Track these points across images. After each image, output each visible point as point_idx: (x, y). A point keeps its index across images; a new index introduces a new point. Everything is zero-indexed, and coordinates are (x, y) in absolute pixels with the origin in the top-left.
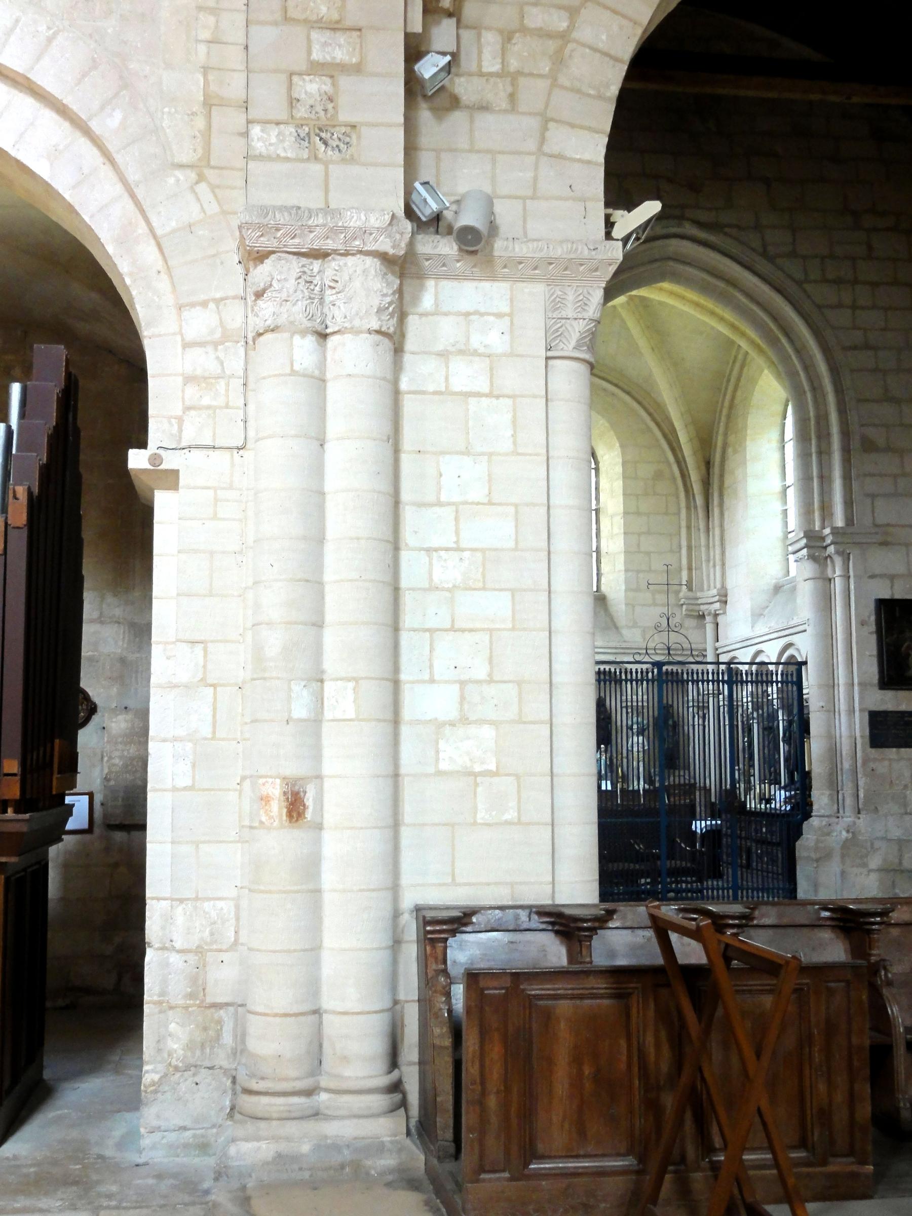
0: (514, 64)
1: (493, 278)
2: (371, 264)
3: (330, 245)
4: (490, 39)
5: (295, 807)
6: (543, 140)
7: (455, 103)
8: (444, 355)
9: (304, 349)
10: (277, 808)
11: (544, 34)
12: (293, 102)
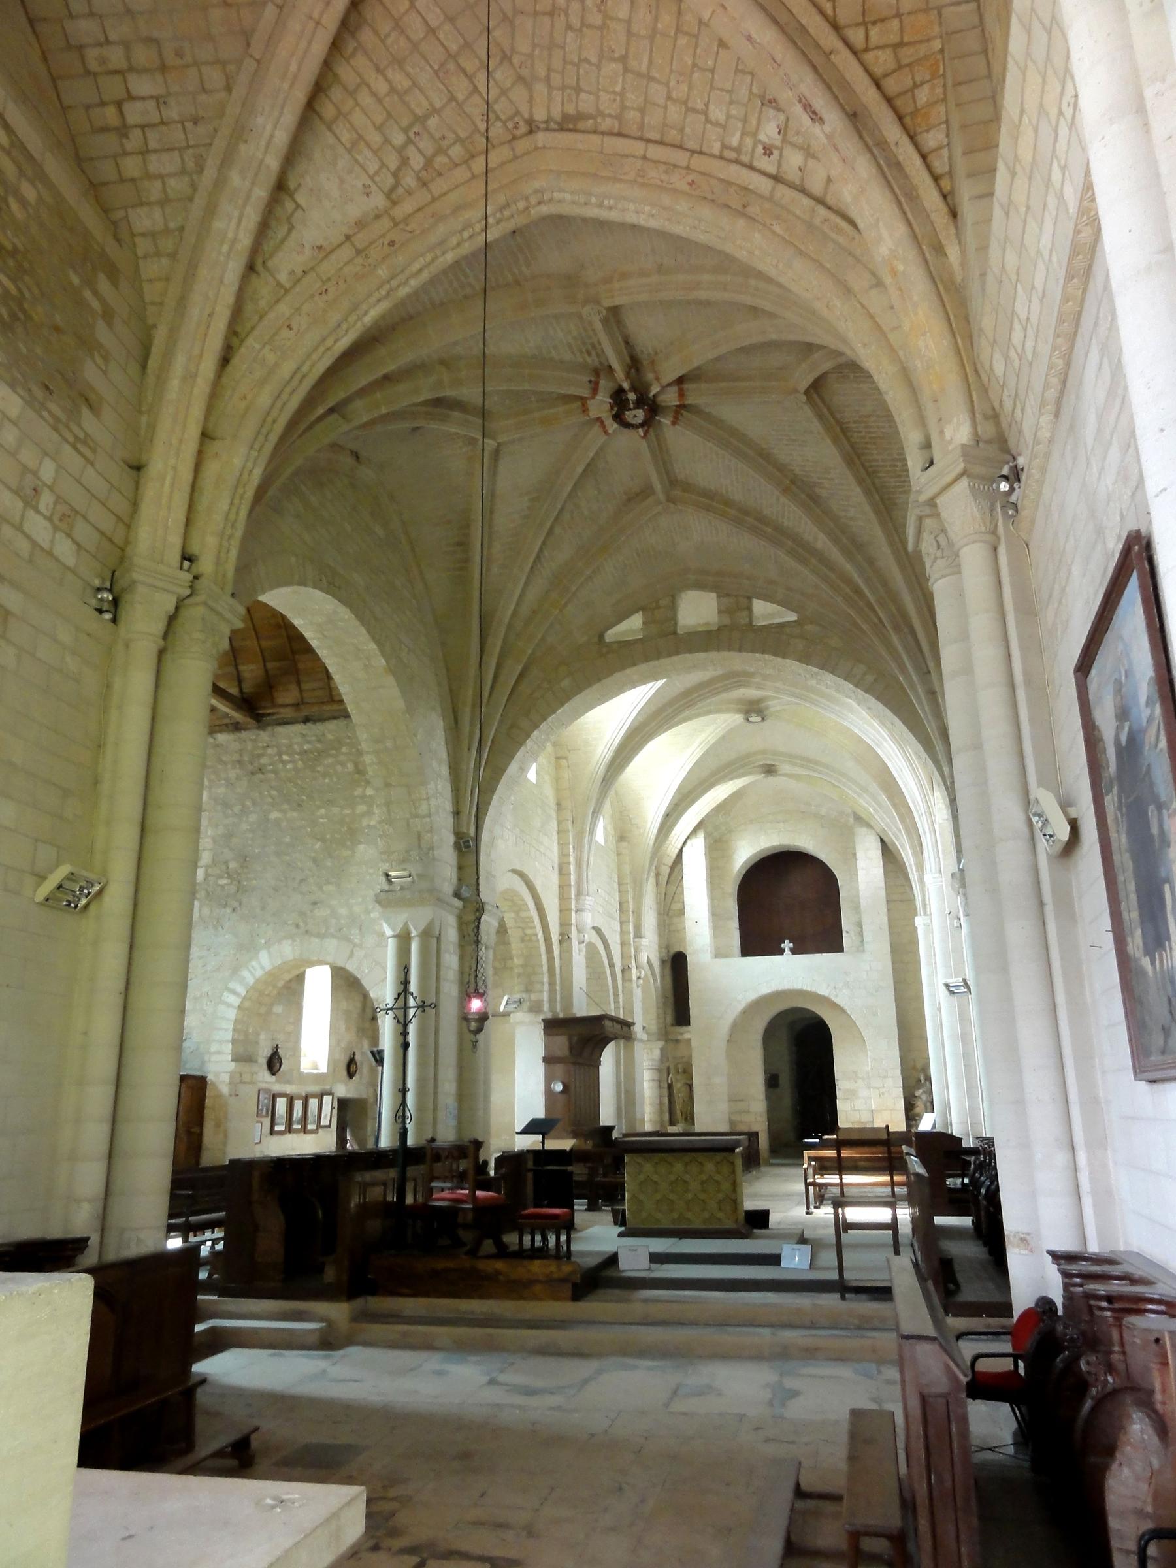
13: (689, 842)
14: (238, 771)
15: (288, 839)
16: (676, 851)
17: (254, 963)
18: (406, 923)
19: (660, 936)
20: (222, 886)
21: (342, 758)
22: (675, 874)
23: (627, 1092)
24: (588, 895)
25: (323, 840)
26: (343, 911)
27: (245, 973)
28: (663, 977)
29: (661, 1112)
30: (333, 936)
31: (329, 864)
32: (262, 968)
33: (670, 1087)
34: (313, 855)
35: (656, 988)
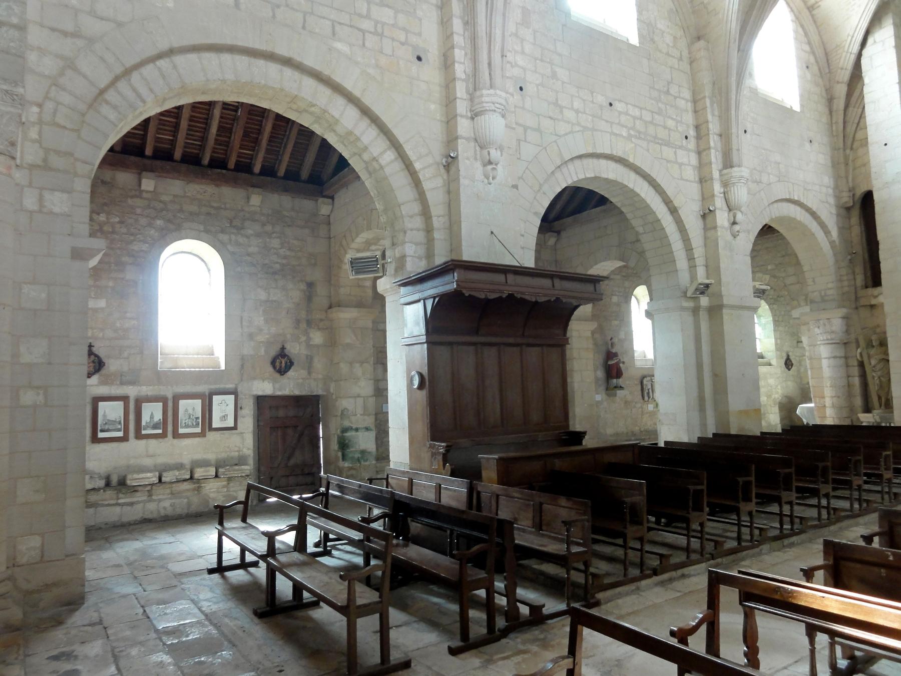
13: (870, 40)
16: (853, 58)
19: (837, 178)
22: (856, 94)
23: (715, 375)
24: (492, 86)
28: (843, 229)
29: (850, 395)
33: (861, 365)
35: (832, 243)
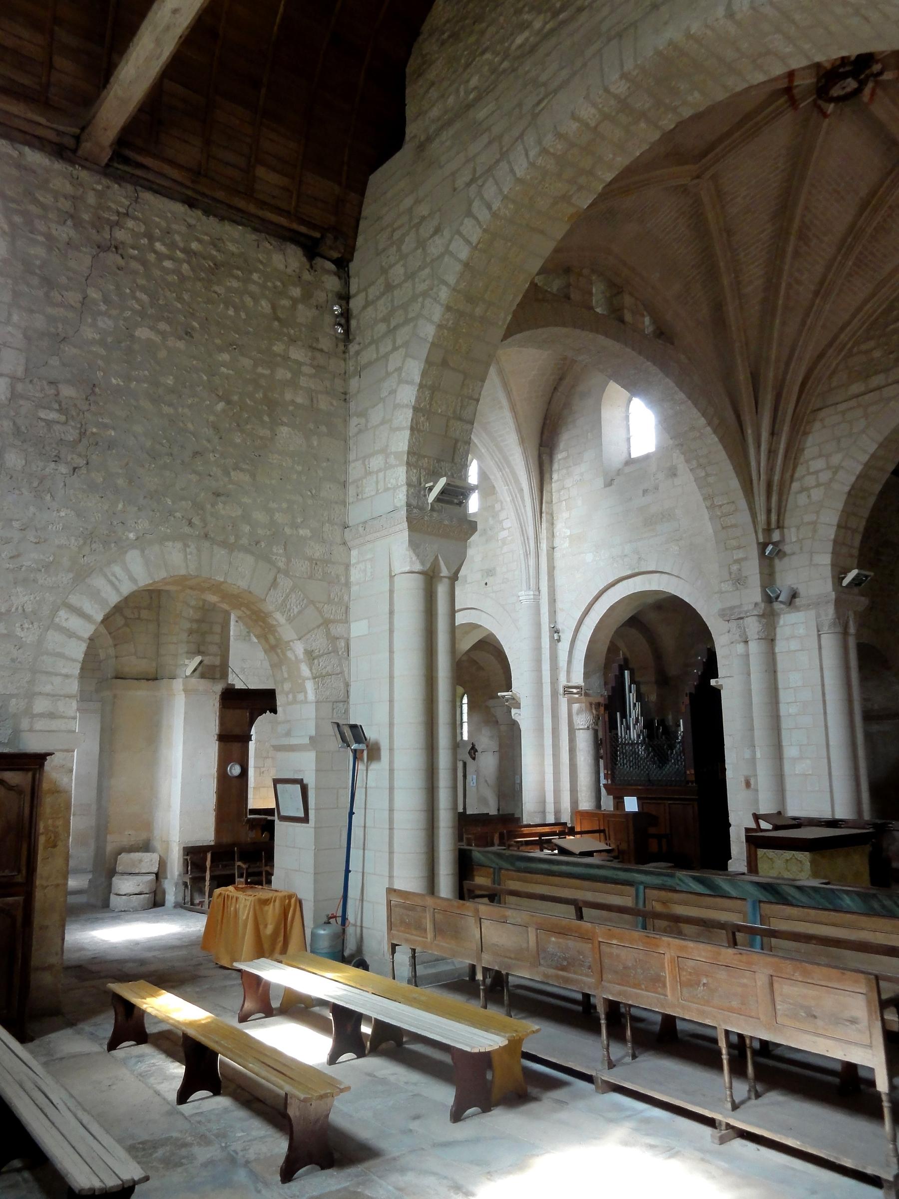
0: (801, 537)
1: (799, 611)
2: (755, 618)
3: (742, 616)
4: (793, 530)
5: (748, 784)
6: (811, 560)
7: (785, 554)
8: (787, 639)
9: (740, 648)
10: (743, 784)
11: (809, 523)
12: (730, 573)
14: (72, 233)
15: (170, 381)
17: (117, 569)
18: (437, 557)
20: (49, 423)
21: (252, 288)
25: (229, 402)
26: (259, 516)
27: (98, 582)
30: (247, 550)
31: (238, 441)
32: (133, 579)
34: (212, 418)
